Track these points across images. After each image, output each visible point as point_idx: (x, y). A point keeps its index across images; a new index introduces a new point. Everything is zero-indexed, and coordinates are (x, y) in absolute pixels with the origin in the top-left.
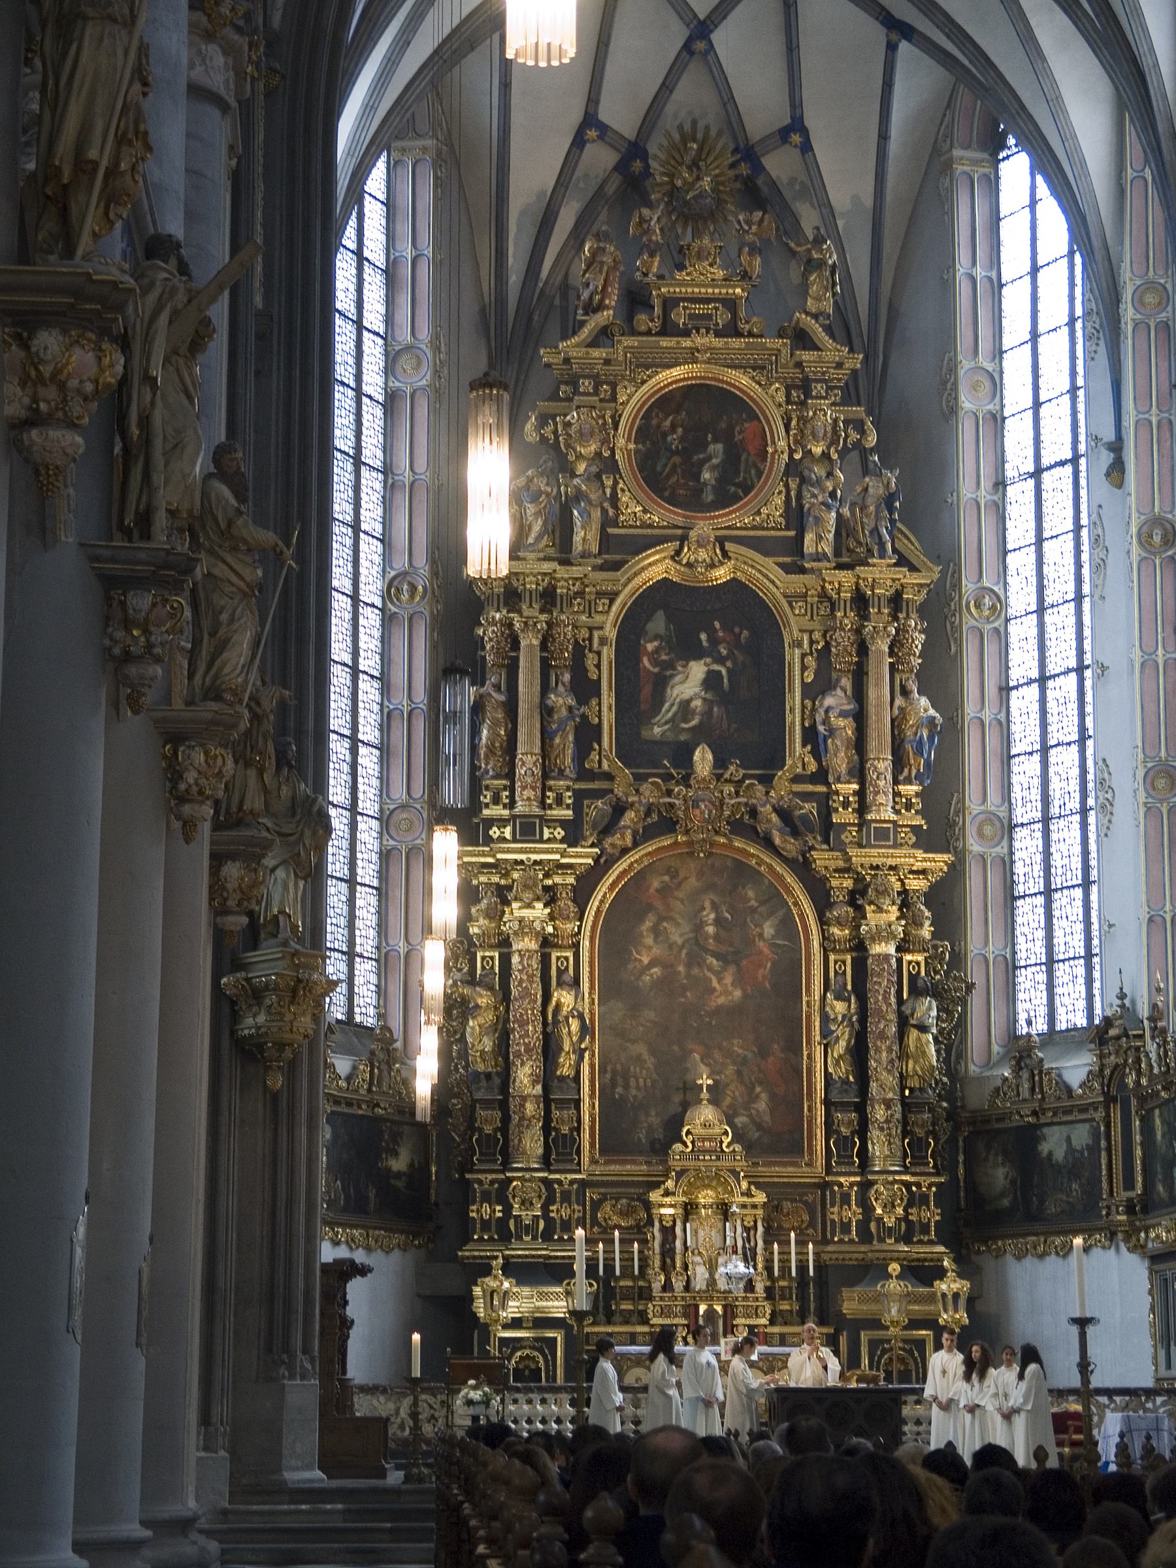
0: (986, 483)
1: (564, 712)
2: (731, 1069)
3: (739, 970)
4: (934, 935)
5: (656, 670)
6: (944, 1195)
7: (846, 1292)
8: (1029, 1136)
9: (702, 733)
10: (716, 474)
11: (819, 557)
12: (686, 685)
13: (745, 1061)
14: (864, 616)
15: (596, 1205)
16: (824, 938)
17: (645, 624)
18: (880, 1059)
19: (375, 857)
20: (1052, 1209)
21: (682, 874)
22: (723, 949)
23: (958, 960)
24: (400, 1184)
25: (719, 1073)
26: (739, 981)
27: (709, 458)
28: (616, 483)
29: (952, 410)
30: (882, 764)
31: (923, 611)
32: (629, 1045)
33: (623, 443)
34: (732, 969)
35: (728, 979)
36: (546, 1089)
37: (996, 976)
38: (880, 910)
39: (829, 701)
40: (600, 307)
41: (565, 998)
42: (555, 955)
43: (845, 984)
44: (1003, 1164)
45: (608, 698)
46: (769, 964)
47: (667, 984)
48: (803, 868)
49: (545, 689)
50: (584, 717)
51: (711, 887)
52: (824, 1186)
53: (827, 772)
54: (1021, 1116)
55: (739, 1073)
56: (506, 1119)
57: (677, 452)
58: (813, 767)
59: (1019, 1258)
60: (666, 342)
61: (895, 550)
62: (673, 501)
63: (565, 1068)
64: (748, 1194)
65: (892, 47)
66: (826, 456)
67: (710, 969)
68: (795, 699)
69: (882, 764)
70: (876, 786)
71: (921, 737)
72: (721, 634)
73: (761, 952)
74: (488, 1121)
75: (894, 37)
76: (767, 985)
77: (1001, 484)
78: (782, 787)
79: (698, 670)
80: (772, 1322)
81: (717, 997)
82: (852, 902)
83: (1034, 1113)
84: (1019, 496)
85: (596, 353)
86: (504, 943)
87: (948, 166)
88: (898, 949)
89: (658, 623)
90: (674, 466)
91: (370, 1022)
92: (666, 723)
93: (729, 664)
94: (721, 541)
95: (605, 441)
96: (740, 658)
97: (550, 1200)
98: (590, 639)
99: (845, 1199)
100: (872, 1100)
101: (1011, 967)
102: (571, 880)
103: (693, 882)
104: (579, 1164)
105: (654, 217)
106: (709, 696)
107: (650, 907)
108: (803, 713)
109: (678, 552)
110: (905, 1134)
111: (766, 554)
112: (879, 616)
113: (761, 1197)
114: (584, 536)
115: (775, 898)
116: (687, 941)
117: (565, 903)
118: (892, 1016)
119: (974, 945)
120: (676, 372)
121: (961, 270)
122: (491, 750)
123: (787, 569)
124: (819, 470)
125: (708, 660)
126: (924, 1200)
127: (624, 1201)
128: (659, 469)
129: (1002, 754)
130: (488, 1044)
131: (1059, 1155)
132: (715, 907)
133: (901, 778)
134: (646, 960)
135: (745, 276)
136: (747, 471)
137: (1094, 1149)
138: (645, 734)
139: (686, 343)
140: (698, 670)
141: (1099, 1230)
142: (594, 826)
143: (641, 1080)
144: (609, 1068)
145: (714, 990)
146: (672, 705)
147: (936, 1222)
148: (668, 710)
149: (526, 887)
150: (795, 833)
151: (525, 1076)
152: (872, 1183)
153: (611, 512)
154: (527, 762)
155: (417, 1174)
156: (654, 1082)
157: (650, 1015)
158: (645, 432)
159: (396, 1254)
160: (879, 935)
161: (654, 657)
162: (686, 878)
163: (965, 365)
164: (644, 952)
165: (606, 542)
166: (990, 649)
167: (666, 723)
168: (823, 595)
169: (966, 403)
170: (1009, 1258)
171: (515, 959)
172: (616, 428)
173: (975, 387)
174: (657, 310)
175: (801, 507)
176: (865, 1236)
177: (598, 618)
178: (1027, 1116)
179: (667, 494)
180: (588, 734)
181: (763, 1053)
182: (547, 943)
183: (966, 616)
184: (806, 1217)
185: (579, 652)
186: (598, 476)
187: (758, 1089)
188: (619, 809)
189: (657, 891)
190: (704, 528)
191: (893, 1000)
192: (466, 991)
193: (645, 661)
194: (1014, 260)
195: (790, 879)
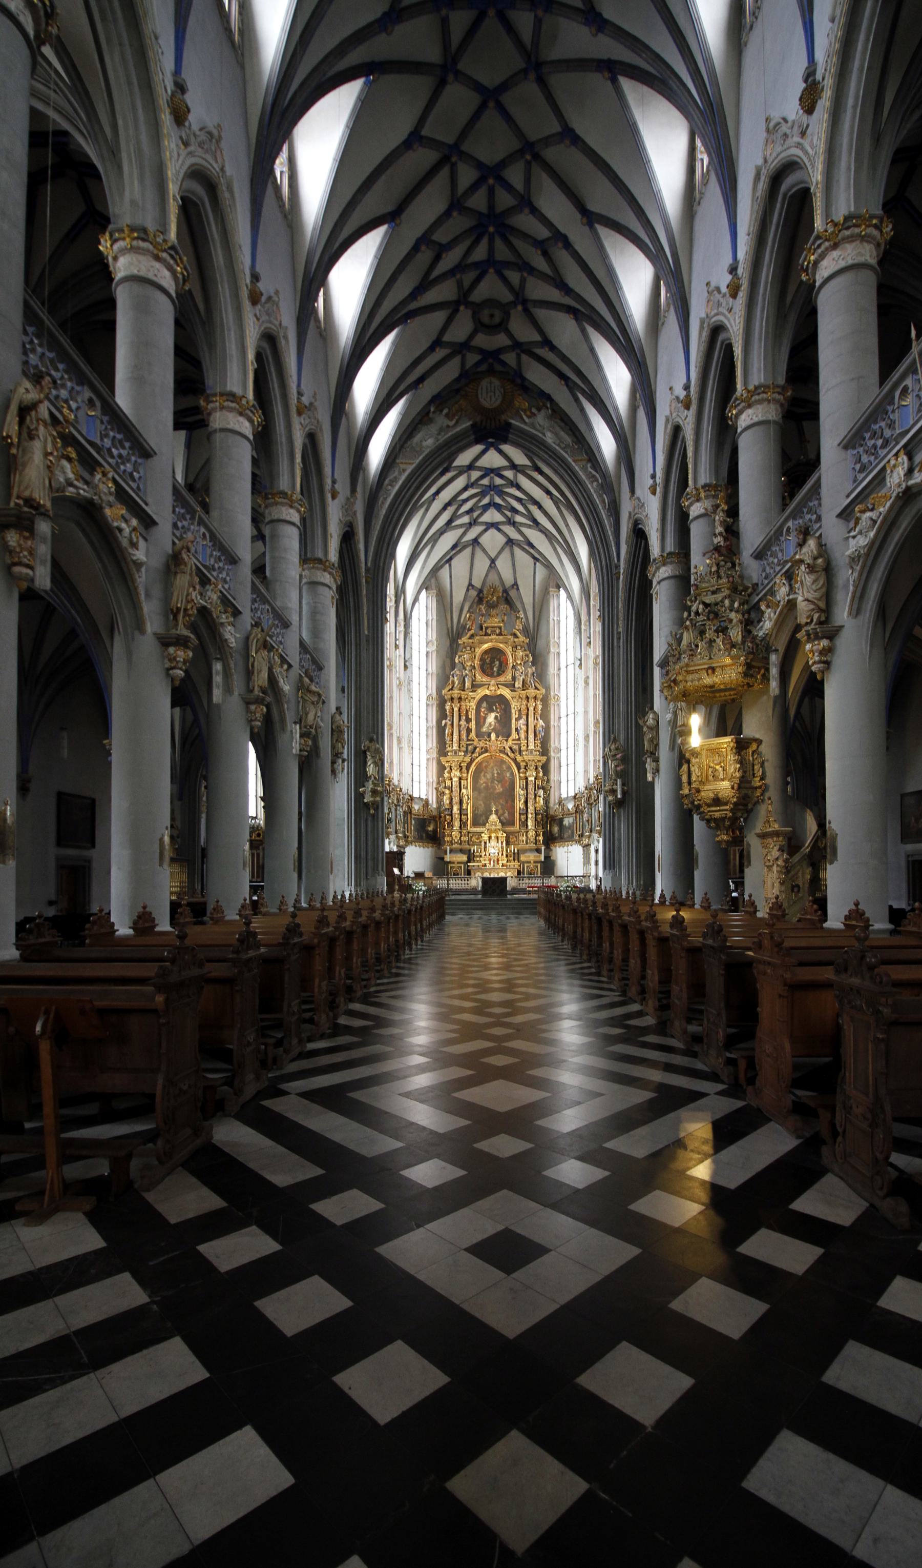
4: (544, 775)
23: (548, 781)
26: (502, 786)
47: (487, 788)
63: (464, 807)
69: (531, 736)
78: (510, 742)
88: (536, 779)
115: (509, 768)
154: (456, 737)
182: (460, 779)
188: (475, 748)
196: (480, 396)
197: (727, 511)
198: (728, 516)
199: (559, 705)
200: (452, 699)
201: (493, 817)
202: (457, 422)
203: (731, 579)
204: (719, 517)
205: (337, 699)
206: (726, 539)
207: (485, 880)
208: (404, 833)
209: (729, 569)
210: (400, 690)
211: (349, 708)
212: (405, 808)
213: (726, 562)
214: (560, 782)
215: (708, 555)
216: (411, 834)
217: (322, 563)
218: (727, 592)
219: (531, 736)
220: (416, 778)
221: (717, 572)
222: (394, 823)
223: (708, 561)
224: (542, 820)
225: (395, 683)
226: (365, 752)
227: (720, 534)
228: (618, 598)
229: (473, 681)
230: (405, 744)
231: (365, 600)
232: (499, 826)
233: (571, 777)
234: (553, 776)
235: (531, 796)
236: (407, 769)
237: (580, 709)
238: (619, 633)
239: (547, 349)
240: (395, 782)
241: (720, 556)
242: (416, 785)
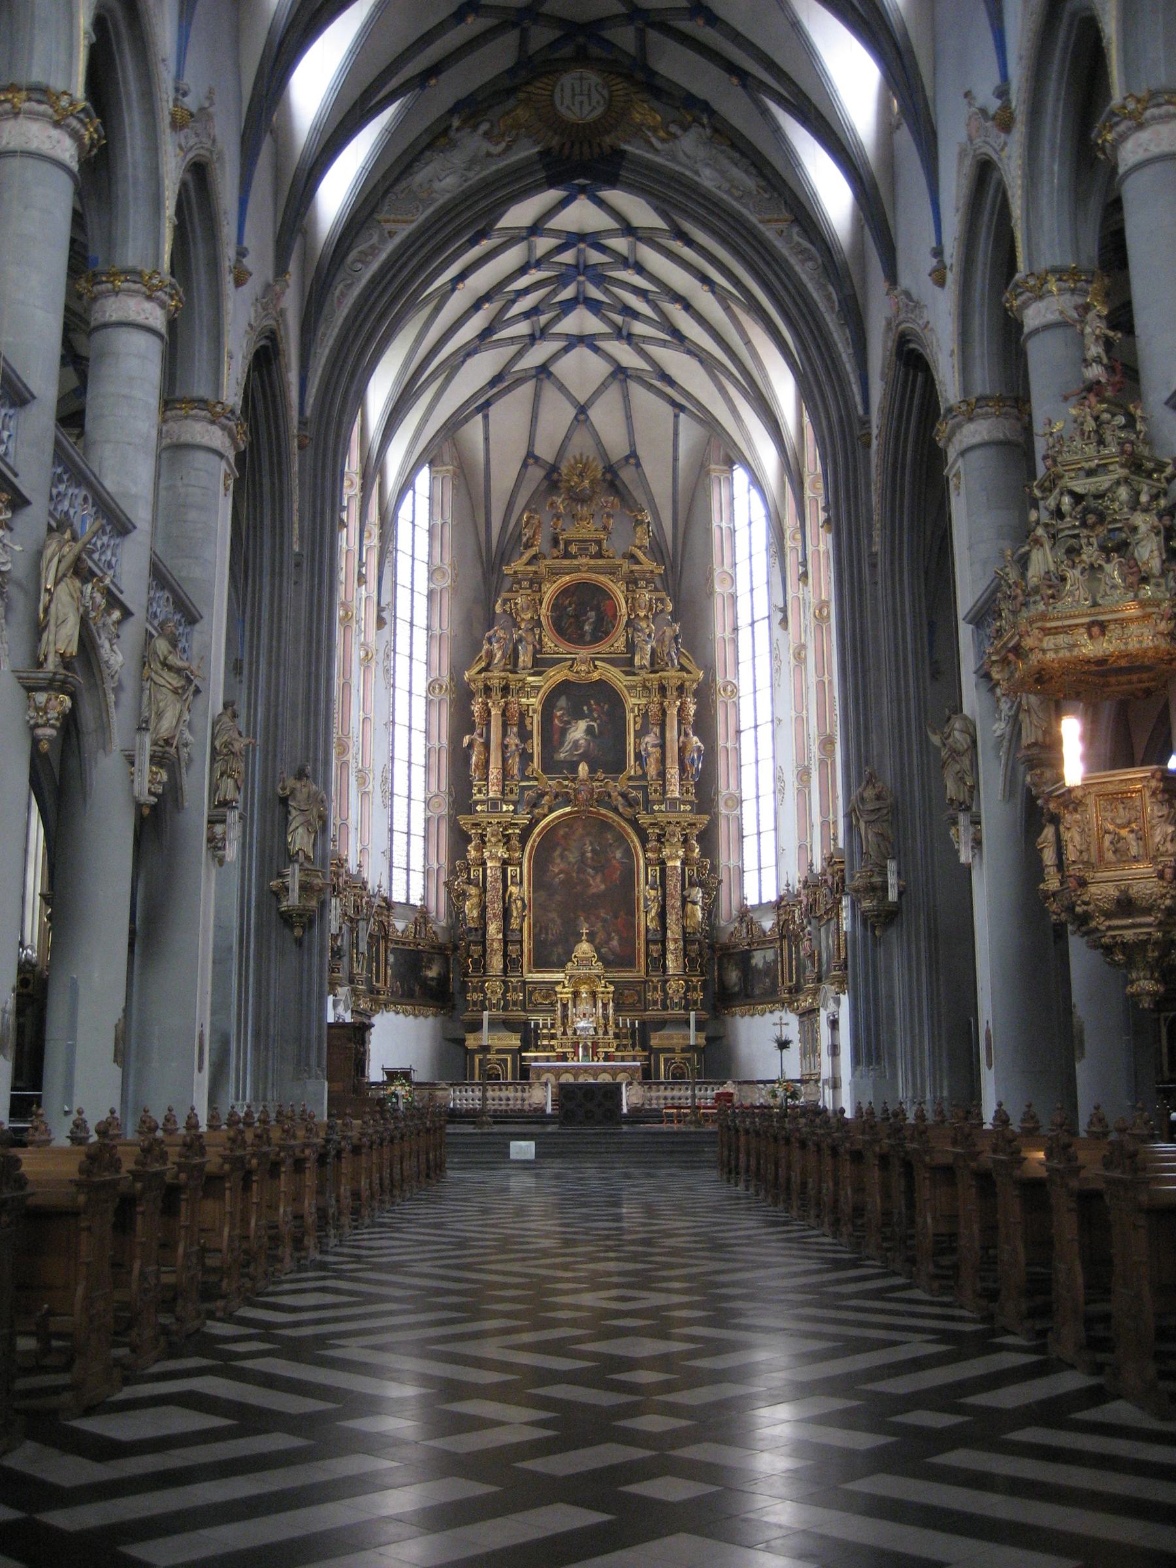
0: (728, 629)
1: (514, 747)
2: (599, 925)
4: (702, 856)
6: (704, 988)
7: (652, 1035)
8: (746, 956)
9: (585, 757)
11: (642, 667)
13: (605, 921)
14: (664, 696)
15: (531, 993)
18: (671, 919)
19: (422, 822)
20: (757, 992)
24: (433, 983)
26: (603, 881)
29: (711, 594)
31: (696, 694)
33: (544, 610)
35: (598, 879)
36: (505, 935)
38: (672, 845)
39: (647, 739)
40: (532, 545)
41: (513, 889)
42: (510, 869)
45: (536, 740)
48: (634, 823)
49: (505, 734)
50: (524, 749)
52: (645, 982)
55: (603, 927)
56: (485, 951)
57: (572, 616)
58: (640, 772)
59: (742, 1016)
60: (566, 562)
61: (679, 663)
64: (606, 987)
65: (676, 416)
66: (646, 617)
68: (631, 738)
74: (475, 950)
75: (677, 411)
77: (736, 629)
80: (617, 1050)
82: (659, 841)
83: (749, 944)
84: (744, 636)
85: (530, 568)
86: (484, 863)
87: (708, 473)
88: (683, 863)
89: (563, 702)
91: (419, 903)
94: (593, 660)
96: (604, 718)
97: (506, 991)
99: (655, 989)
102: (517, 831)
103: (580, 831)
105: (559, 501)
107: (558, 844)
109: (572, 666)
110: (685, 955)
111: (615, 666)
113: (611, 988)
114: (525, 658)
115: (621, 839)
117: (515, 842)
118: (679, 897)
119: (723, 860)
121: (714, 524)
122: (477, 766)
123: (627, 673)
124: (643, 624)
126: (695, 989)
130: (475, 913)
131: (760, 965)
132: (591, 844)
134: (556, 870)
135: (605, 528)
137: (775, 961)
139: (576, 562)
140: (582, 725)
141: (777, 1002)
142: (528, 803)
148: (567, 746)
149: (493, 835)
150: (630, 805)
151: (493, 929)
152: (666, 981)
154: (494, 773)
155: (443, 979)
157: (558, 898)
158: (556, 606)
160: (670, 858)
163: (717, 571)
165: (536, 662)
166: (731, 712)
168: (645, 687)
169: (718, 588)
170: (738, 1017)
171: (489, 871)
172: (541, 604)
173: (722, 581)
174: (562, 546)
175: (633, 642)
176: (665, 1007)
177: (532, 700)
180: (526, 757)
181: (616, 917)
182: (505, 863)
183: (719, 696)
185: (522, 716)
186: (532, 629)
190: (584, 653)
191: (679, 889)
192: (465, 887)
194: (740, 521)
195: (630, 830)
196: (558, 102)
197: (1107, 317)
198: (1112, 327)
199: (736, 705)
200: (487, 690)
201: (584, 948)
202: (508, 148)
203: (1128, 447)
204: (1095, 326)
205: (228, 687)
206: (1111, 369)
207: (565, 1093)
208: (369, 981)
209: (1122, 428)
210: (367, 668)
211: (251, 705)
212: (373, 927)
213: (1114, 415)
214: (741, 872)
215: (1074, 400)
216: (387, 981)
217: (209, 408)
218: (1122, 472)
219: (673, 772)
220: (399, 859)
221: (1097, 432)
222: (346, 959)
223: (1073, 412)
224: (700, 955)
225: (357, 654)
226: (284, 801)
227: (1097, 360)
228: (868, 485)
230: (374, 785)
231: (296, 482)
232: (598, 969)
233: (769, 858)
234: (725, 859)
235: (675, 902)
236: (378, 843)
237: (787, 713)
238: (873, 555)
239: (701, 22)
240: (352, 866)
241: (1101, 402)
242: (399, 876)
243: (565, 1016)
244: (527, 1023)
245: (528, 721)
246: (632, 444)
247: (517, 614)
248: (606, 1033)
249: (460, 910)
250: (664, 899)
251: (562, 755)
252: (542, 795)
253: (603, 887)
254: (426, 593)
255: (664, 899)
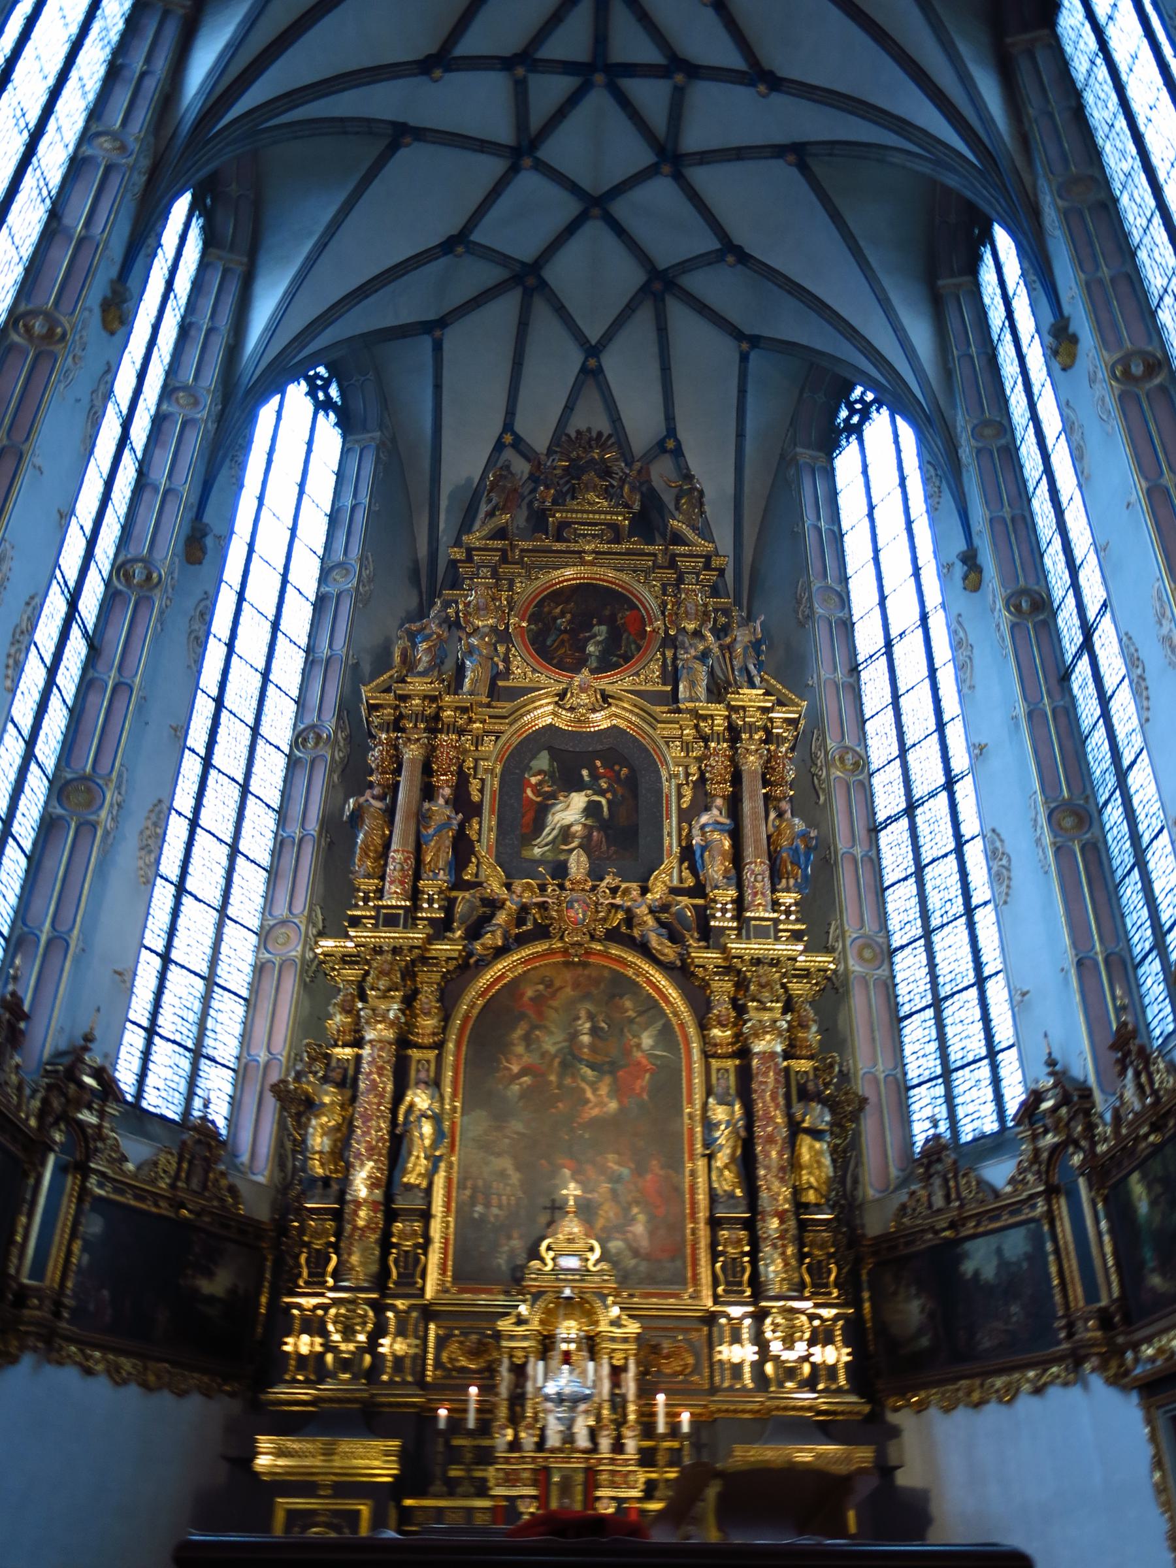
2: (605, 1187)
3: (615, 1080)
5: (539, 799)
10: (600, 648)
12: (566, 813)
13: (616, 1179)
16: (705, 1044)
17: (531, 760)
21: (557, 983)
22: (599, 1059)
25: (592, 1191)
26: (617, 1091)
27: (595, 636)
28: (508, 650)
30: (756, 868)
32: (492, 1158)
34: (608, 1079)
35: (604, 1090)
37: (887, 1095)
43: (728, 1088)
44: (917, 1296)
46: (647, 1076)
48: (681, 972)
51: (587, 996)
52: (710, 1319)
53: (704, 886)
54: (936, 1232)
55: (614, 1194)
57: (565, 631)
58: (690, 882)
59: (947, 1410)
62: (561, 666)
67: (584, 1079)
68: (671, 824)
70: (754, 887)
71: (797, 847)
72: (602, 771)
73: (639, 1063)
76: (645, 1097)
79: (579, 801)
81: (591, 1109)
90: (563, 642)
92: (547, 845)
93: (609, 795)
95: (501, 619)
98: (475, 768)
100: (762, 1213)
101: (903, 1089)
104: (423, 1289)
106: (589, 822)
107: (522, 1016)
108: (680, 835)
110: (801, 1257)
112: (751, 743)
115: (651, 1008)
116: (559, 1051)
120: (569, 572)
125: (589, 792)
127: (474, 1337)
128: (549, 643)
129: (876, 886)
132: (591, 1017)
133: (779, 887)
134: (515, 1069)
136: (628, 645)
138: (526, 854)
140: (579, 801)
143: (504, 1198)
144: (469, 1184)
145: (587, 1101)
146: (553, 829)
147: (847, 1364)
148: (549, 834)
153: (501, 666)
156: (519, 1199)
159: (194, 1404)
161: (536, 789)
162: (561, 988)
164: (514, 1060)
167: (547, 845)
178: (944, 1230)
179: (555, 661)
184: (691, 1360)
187: (635, 1210)
189: (531, 999)
193: (529, 792)
229: (496, 676)
243: (518, 1399)
244: (427, 1416)
245: (475, 784)
246: (670, 418)
247: (468, 622)
248: (618, 1447)
249: (301, 1146)
250: (749, 1126)
251: (537, 851)
252: (494, 905)
253: (613, 1105)
254: (313, 598)
255: (749, 1126)
